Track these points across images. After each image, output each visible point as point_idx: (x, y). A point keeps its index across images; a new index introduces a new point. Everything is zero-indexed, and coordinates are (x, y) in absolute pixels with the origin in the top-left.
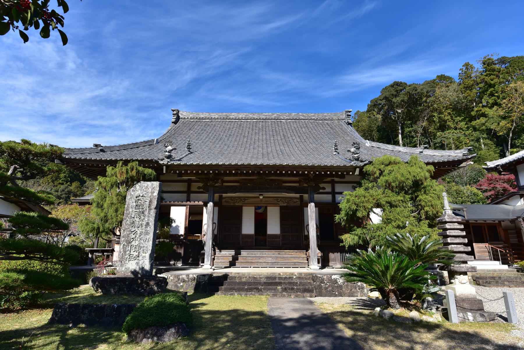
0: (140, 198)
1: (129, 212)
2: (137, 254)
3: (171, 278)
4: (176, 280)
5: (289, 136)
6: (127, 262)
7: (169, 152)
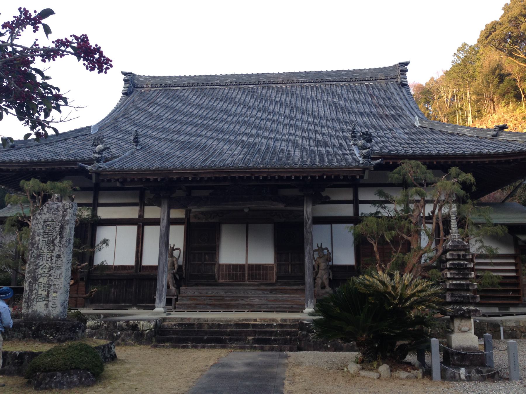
0: (48, 223)
1: (36, 241)
2: (46, 293)
3: (105, 325)
4: (112, 327)
5: (299, 111)
6: (34, 303)
7: (99, 153)
